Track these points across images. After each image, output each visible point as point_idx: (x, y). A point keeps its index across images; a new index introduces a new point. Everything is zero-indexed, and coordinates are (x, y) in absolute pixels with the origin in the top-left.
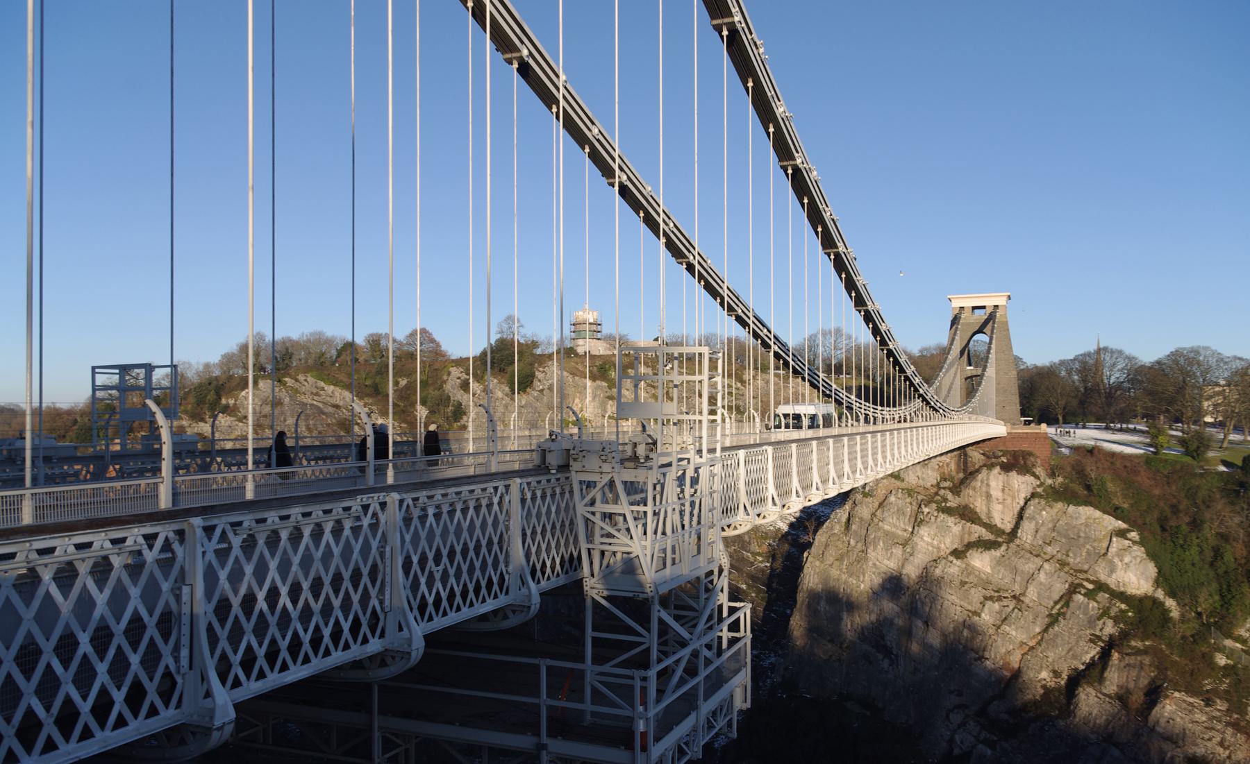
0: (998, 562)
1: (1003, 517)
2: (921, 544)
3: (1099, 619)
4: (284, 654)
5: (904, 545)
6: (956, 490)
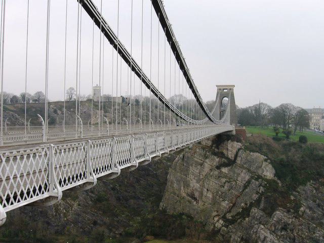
0: (229, 170)
1: (231, 155)
2: (206, 164)
3: (259, 187)
4: (19, 197)
5: (201, 165)
6: (217, 147)
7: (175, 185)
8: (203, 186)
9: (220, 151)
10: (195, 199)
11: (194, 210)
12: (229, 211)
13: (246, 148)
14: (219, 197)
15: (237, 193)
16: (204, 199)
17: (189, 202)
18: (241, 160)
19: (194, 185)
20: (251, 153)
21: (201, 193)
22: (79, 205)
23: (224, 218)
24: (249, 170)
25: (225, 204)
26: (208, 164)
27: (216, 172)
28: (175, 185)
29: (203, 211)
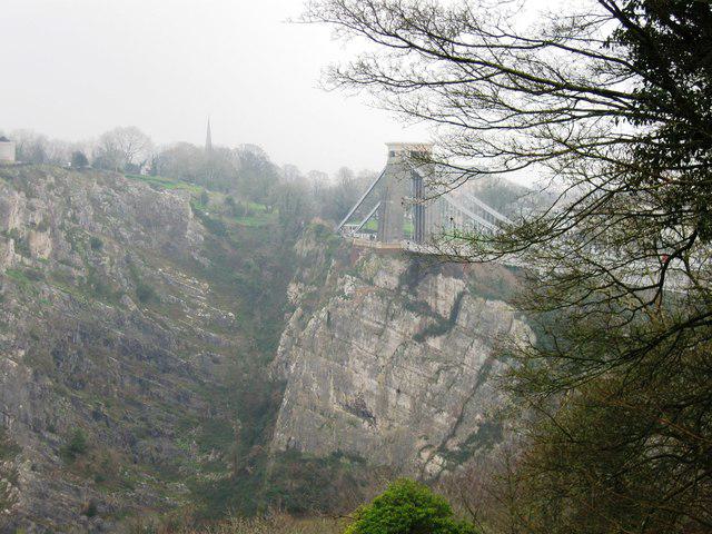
0: (445, 343)
6: (412, 288)
7: (315, 385)
8: (387, 383)
9: (419, 299)
10: (367, 415)
11: (366, 441)
12: (453, 435)
13: (476, 292)
14: (428, 405)
15: (464, 393)
16: (391, 413)
17: (352, 423)
18: (468, 319)
19: (364, 381)
20: (488, 302)
21: (384, 401)
22: (33, 468)
23: (442, 450)
24: (485, 340)
25: (442, 420)
26: (395, 334)
27: (417, 350)
28: (315, 387)
29: (388, 441)
